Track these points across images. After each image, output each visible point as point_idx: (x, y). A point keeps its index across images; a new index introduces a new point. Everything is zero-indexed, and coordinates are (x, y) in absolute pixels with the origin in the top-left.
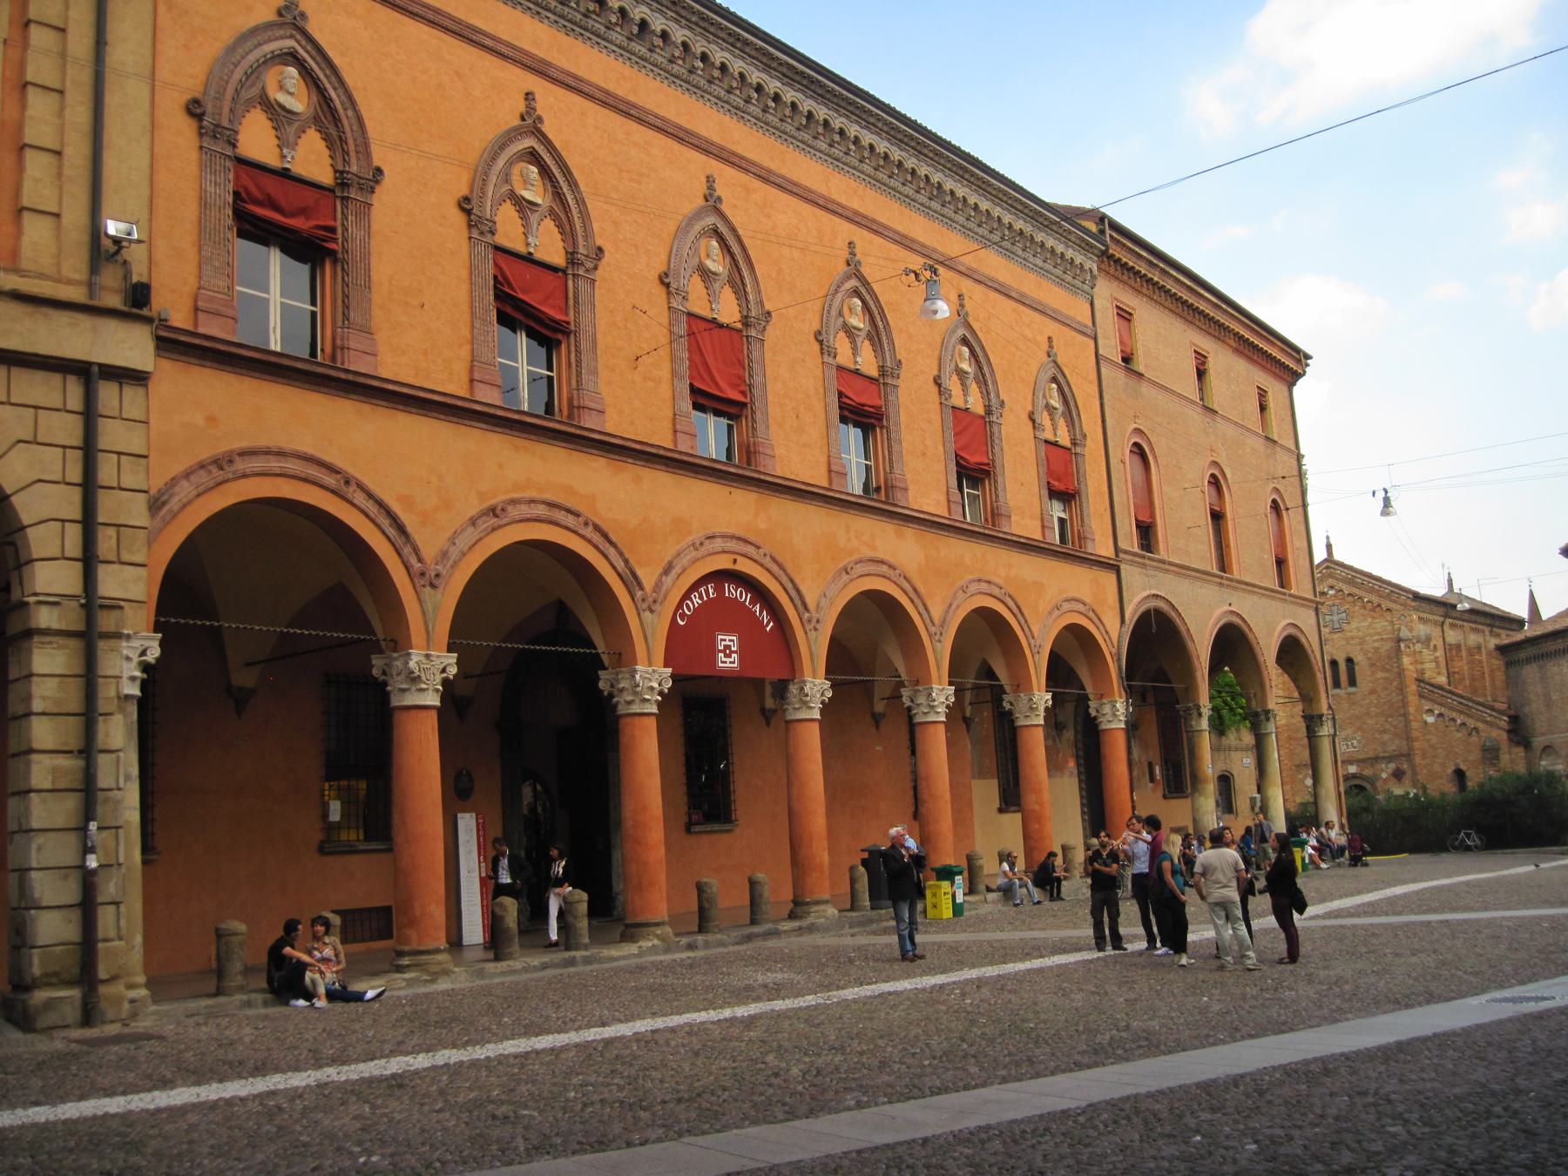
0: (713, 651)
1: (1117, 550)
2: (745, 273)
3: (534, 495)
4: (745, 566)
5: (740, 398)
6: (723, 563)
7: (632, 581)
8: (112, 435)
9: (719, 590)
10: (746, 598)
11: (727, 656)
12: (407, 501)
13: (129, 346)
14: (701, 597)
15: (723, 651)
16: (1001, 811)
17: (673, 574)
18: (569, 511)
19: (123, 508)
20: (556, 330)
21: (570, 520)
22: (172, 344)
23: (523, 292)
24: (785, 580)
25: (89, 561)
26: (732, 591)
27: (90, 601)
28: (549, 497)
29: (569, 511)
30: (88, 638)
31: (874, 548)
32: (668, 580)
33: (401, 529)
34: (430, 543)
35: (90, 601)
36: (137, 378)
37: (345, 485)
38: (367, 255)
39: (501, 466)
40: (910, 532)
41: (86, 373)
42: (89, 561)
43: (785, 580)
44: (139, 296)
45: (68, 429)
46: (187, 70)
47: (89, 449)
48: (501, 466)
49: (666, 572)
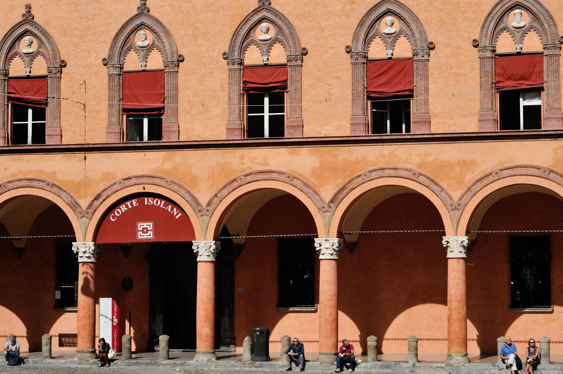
2: (165, 40)
3: (22, 177)
7: (75, 206)
10: (161, 203)
11: (144, 232)
14: (127, 206)
15: (143, 231)
17: (100, 200)
18: (40, 181)
20: (41, 104)
21: (41, 184)
23: (26, 92)
24: (182, 192)
28: (29, 177)
29: (40, 181)
31: (267, 165)
32: (97, 203)
39: (6, 169)
40: (305, 150)
43: (182, 192)
48: (6, 169)
49: (96, 199)
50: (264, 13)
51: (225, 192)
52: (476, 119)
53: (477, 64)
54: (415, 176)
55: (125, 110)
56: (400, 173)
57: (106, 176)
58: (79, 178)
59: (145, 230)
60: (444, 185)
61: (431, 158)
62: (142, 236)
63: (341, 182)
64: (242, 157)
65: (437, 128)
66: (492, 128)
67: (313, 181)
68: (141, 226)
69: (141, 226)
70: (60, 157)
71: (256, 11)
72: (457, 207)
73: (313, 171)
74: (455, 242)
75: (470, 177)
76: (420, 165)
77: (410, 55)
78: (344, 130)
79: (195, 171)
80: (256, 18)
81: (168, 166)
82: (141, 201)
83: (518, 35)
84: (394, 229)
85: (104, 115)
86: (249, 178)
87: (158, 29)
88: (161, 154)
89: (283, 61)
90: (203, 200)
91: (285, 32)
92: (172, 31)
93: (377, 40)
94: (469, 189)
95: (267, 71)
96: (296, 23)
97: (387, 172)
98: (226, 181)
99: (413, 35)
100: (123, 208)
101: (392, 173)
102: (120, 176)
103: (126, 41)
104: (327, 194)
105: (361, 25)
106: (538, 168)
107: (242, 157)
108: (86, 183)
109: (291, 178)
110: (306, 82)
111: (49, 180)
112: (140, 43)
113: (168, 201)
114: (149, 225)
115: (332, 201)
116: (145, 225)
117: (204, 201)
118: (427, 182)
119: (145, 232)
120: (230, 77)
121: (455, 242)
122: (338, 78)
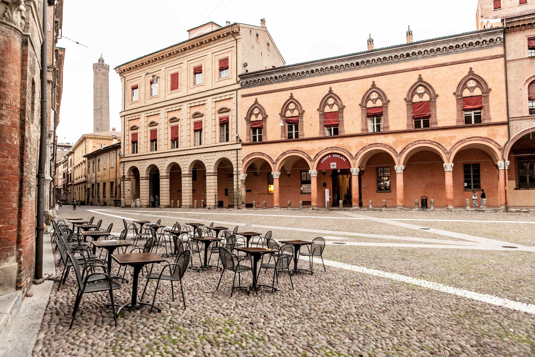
0: (330, 166)
1: (508, 118)
4: (335, 151)
5: (337, 123)
6: (331, 152)
7: (309, 158)
8: (239, 155)
9: (332, 156)
10: (339, 156)
12: (272, 155)
13: (239, 146)
16: (516, 189)
19: (240, 162)
22: (243, 145)
25: (237, 167)
26: (334, 156)
27: (237, 171)
30: (237, 175)
33: (271, 158)
34: (275, 159)
35: (237, 171)
36: (241, 149)
37: (263, 154)
38: (266, 127)
40: (390, 136)
41: (237, 150)
42: (237, 167)
44: (240, 141)
45: (235, 155)
46: (245, 115)
47: (237, 157)
50: (374, 89)
51: (362, 151)
52: (455, 121)
53: (455, 101)
54: (432, 142)
55: (325, 126)
56: (426, 142)
57: (319, 148)
58: (310, 149)
59: (333, 165)
60: (443, 145)
61: (438, 136)
62: (332, 167)
63: (404, 146)
64: (367, 139)
65: (440, 125)
66: (462, 124)
67: (393, 146)
68: (332, 164)
69: (332, 164)
70: (304, 142)
71: (370, 89)
72: (449, 153)
73: (393, 143)
74: (448, 166)
75: (454, 142)
76: (434, 139)
77: (429, 100)
78: (404, 127)
79: (350, 145)
80: (371, 91)
81: (341, 143)
82: (332, 156)
83: (472, 90)
84: (424, 162)
85: (318, 128)
86: (370, 146)
87: (336, 98)
88: (338, 140)
89: (381, 105)
90: (354, 155)
91: (382, 95)
92: (341, 98)
93: (416, 96)
94: (454, 146)
95: (375, 109)
96: (385, 92)
97: (421, 142)
98: (362, 147)
99: (430, 92)
100: (326, 158)
101: (423, 142)
102: (324, 148)
103: (325, 103)
104: (399, 150)
105: (410, 90)
106: (481, 137)
107: (367, 139)
108: (313, 150)
109: (385, 145)
110: (390, 112)
111: (300, 150)
112: (330, 103)
113: (341, 155)
114: (335, 164)
115: (401, 153)
116: (333, 163)
117: (354, 155)
118: (437, 144)
119: (333, 165)
120: (362, 112)
121: (448, 166)
122: (401, 110)
